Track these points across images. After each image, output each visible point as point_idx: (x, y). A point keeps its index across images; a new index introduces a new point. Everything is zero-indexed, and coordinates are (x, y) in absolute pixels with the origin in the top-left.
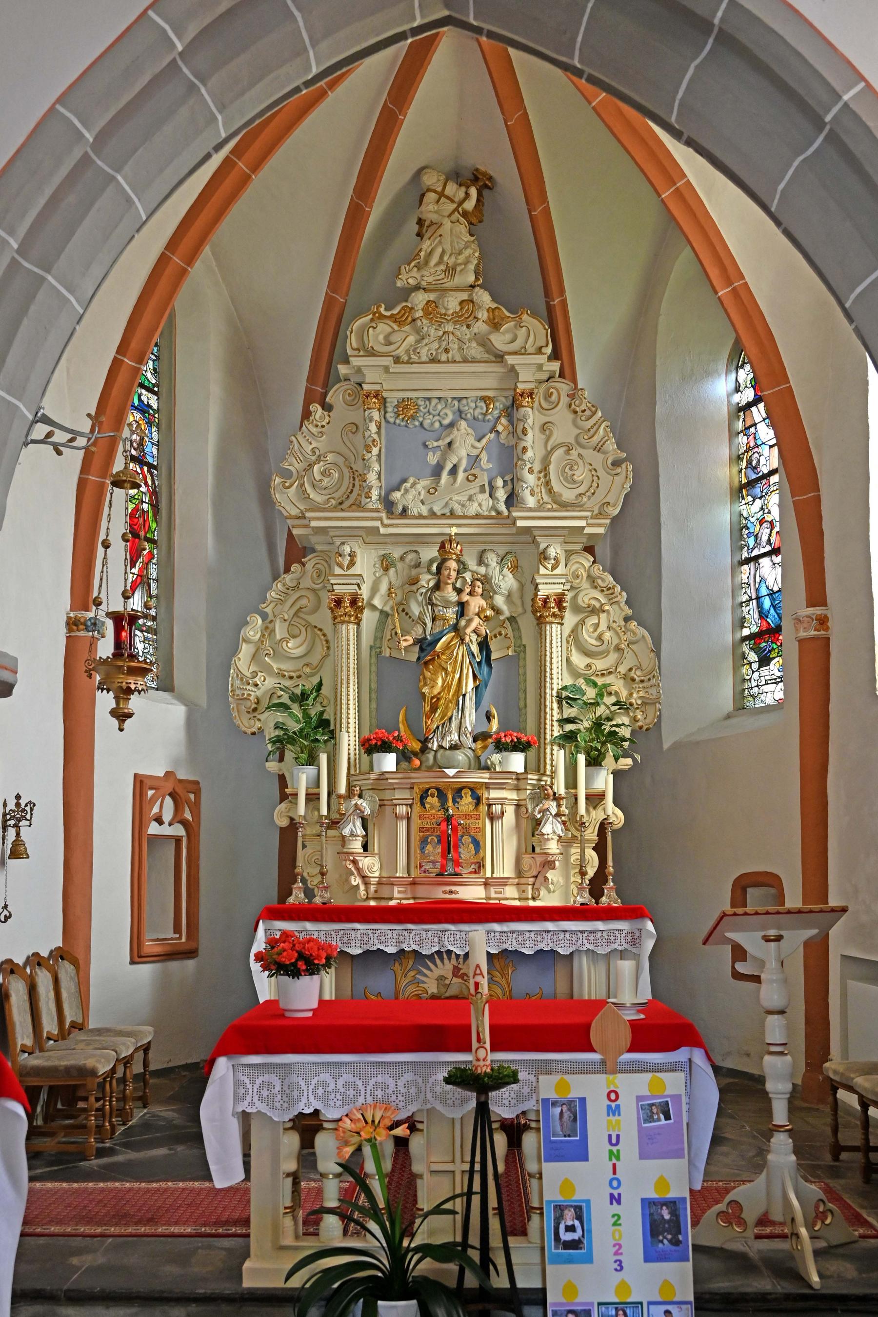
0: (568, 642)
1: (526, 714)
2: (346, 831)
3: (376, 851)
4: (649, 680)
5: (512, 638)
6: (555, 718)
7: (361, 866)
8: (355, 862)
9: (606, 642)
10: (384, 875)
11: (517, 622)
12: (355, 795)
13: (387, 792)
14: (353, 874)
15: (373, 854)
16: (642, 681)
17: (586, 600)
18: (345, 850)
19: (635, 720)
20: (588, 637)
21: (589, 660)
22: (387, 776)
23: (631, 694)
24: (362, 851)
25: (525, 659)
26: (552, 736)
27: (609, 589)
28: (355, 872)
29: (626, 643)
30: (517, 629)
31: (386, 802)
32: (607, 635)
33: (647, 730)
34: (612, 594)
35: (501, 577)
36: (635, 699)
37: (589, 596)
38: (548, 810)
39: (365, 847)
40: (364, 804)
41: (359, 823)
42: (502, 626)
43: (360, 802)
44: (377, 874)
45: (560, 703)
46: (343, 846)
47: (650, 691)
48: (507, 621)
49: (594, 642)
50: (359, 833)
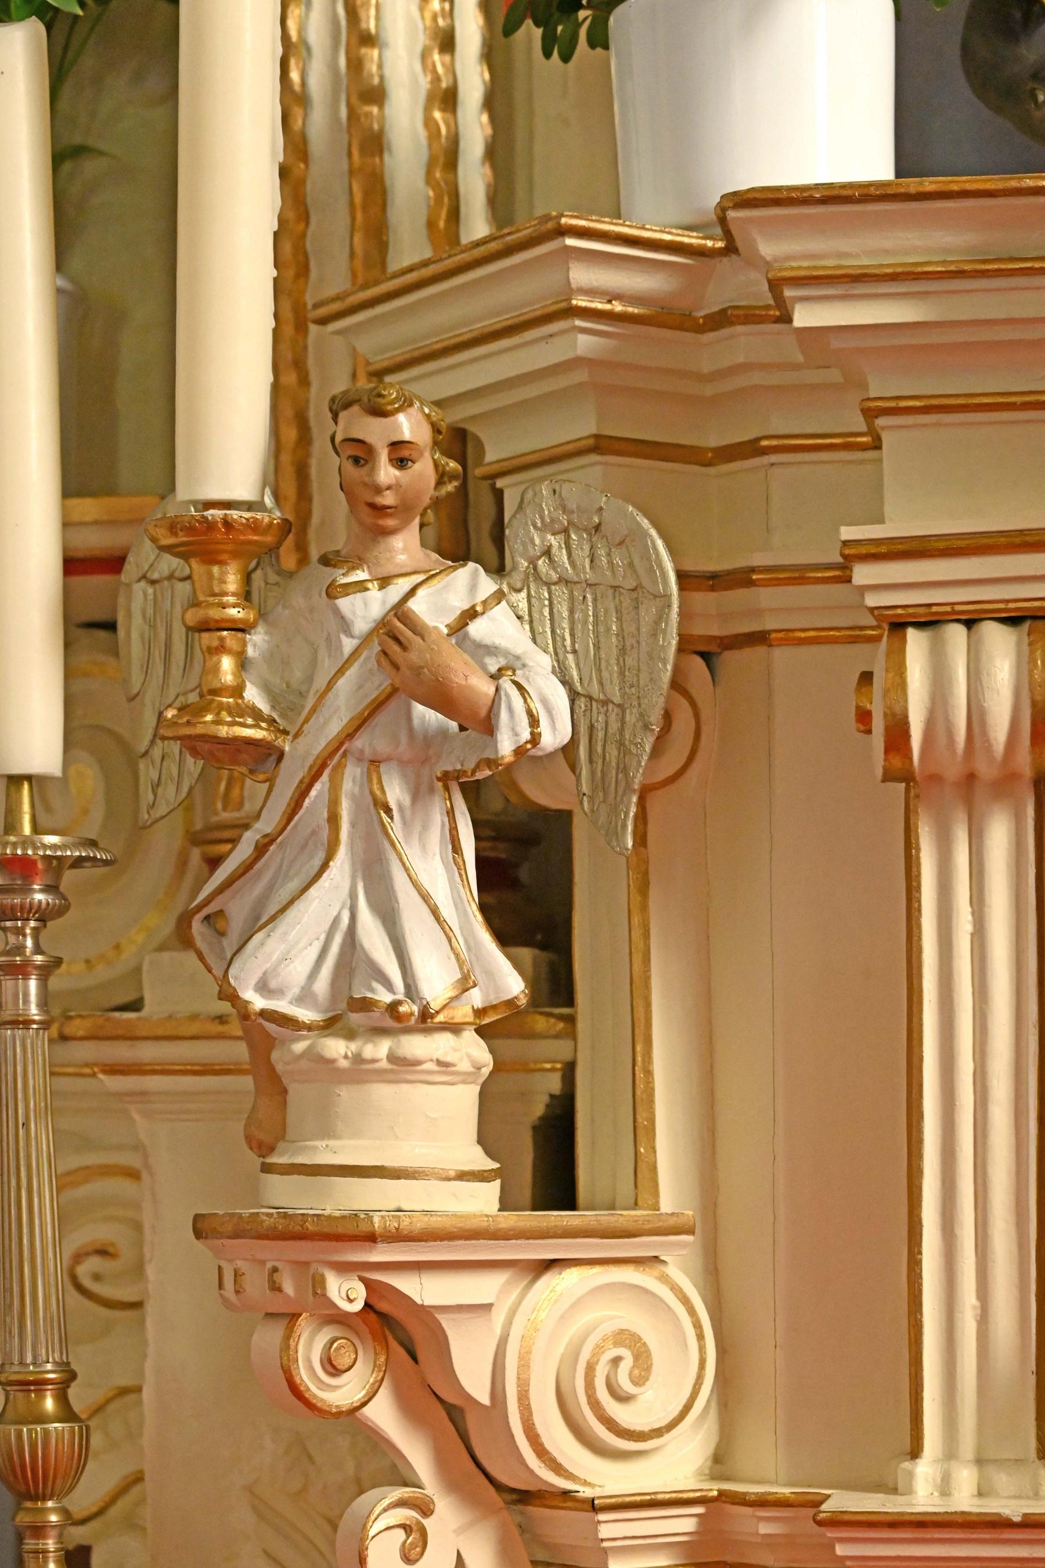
2: (285, 964)
3: (673, 1193)
7: (474, 1379)
8: (396, 1332)
10: (767, 1472)
12: (375, 519)
13: (786, 475)
14: (398, 1474)
15: (631, 1240)
18: (286, 1195)
22: (776, 246)
24: (482, 1201)
28: (418, 1456)
31: (772, 607)
39: (549, 1161)
40: (501, 628)
41: (437, 866)
43: (445, 596)
44: (678, 1465)
46: (265, 1141)
50: (436, 982)
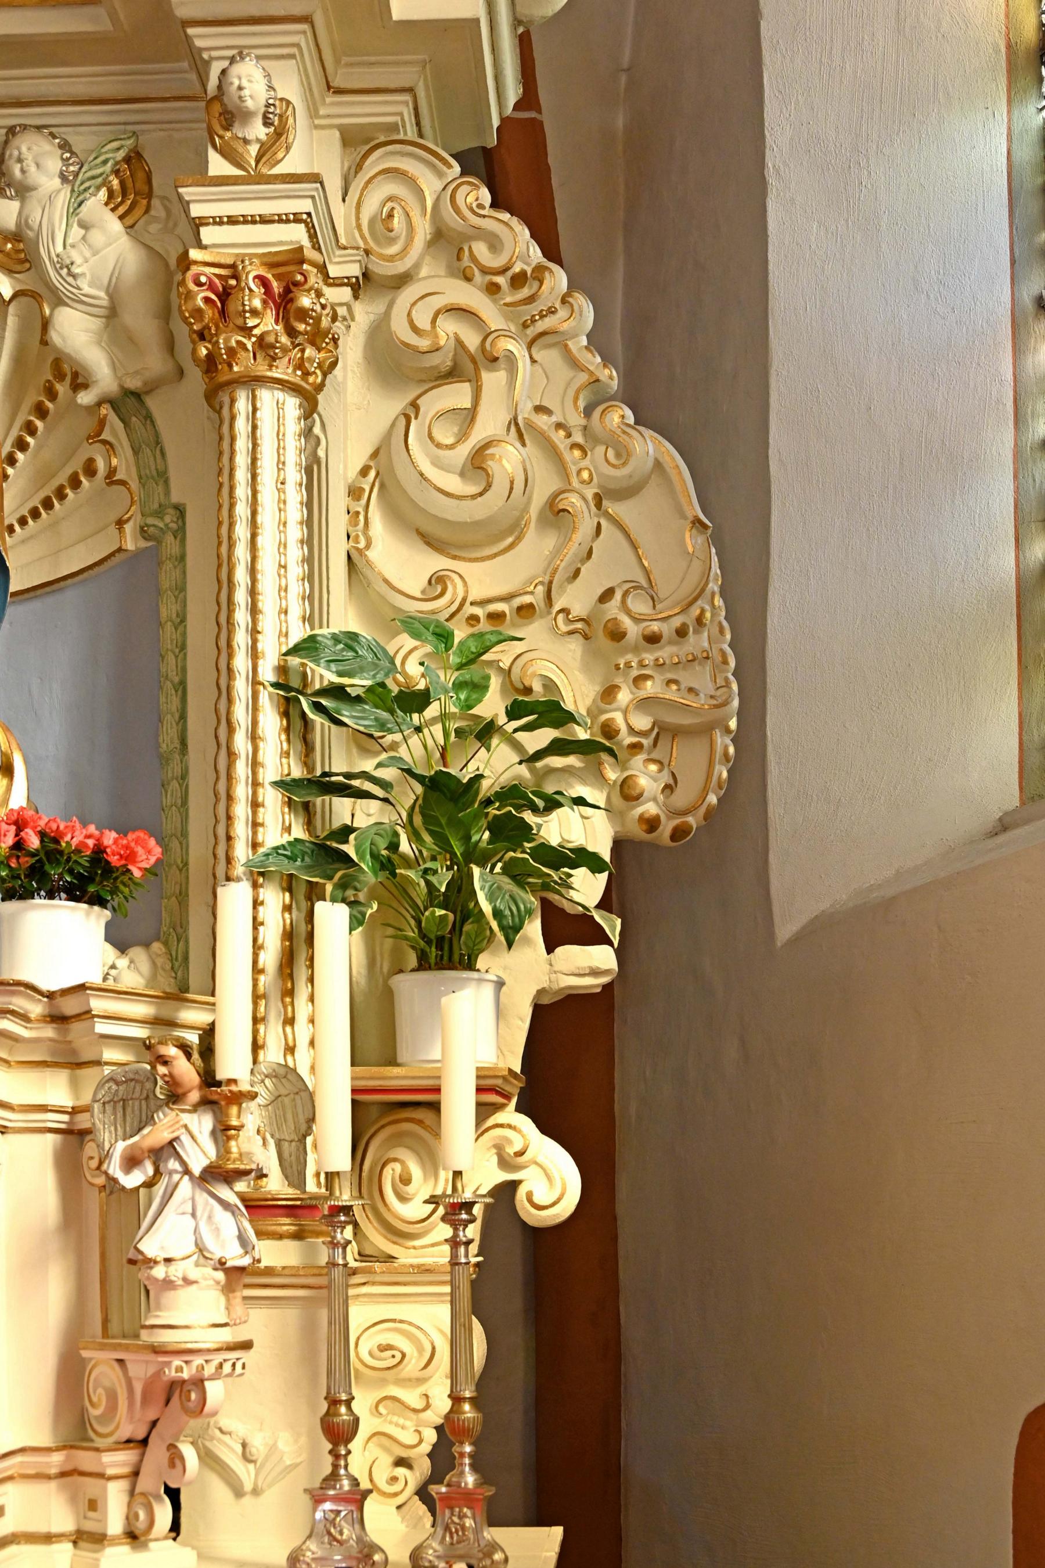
0: (355, 492)
1: (184, 776)
4: (681, 632)
5: (134, 485)
6: (270, 773)
9: (500, 487)
11: (149, 417)
16: (653, 639)
17: (423, 321)
19: (628, 792)
20: (435, 470)
21: (438, 563)
23: (609, 693)
25: (182, 558)
26: (255, 845)
27: (518, 281)
29: (589, 493)
30: (149, 444)
32: (509, 459)
33: (677, 834)
34: (531, 299)
35: (76, 232)
36: (628, 718)
37: (432, 306)
38: (171, 1147)
42: (95, 436)
45: (288, 708)
47: (687, 679)
48: (113, 418)
49: (453, 483)
